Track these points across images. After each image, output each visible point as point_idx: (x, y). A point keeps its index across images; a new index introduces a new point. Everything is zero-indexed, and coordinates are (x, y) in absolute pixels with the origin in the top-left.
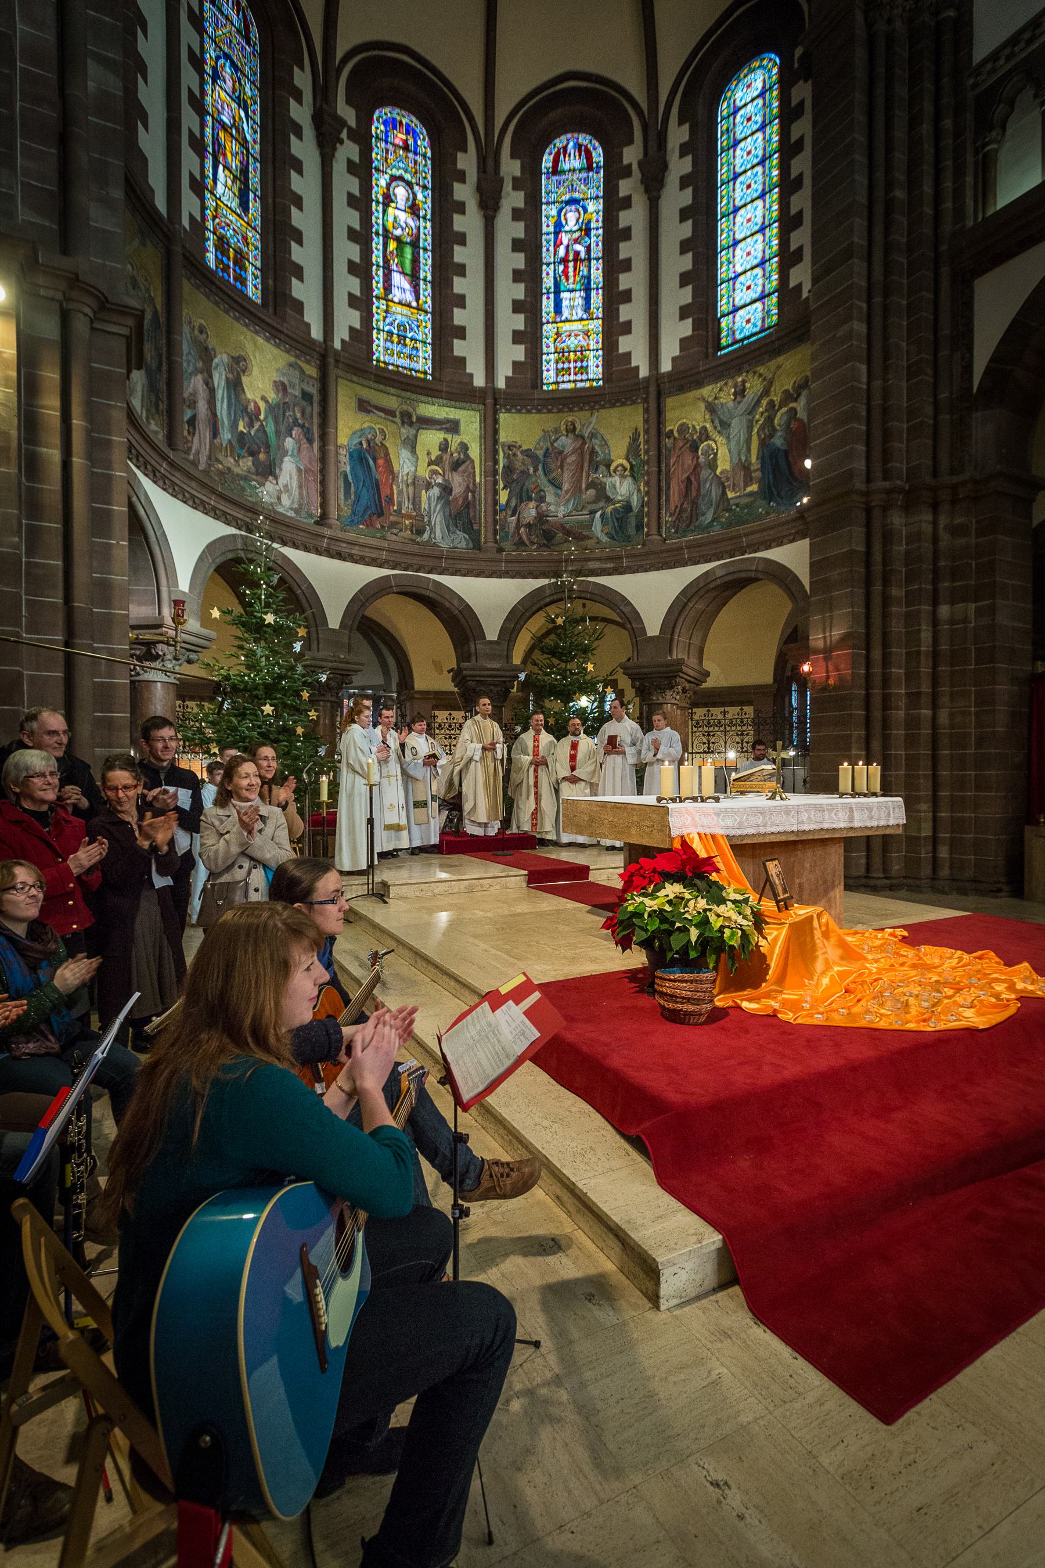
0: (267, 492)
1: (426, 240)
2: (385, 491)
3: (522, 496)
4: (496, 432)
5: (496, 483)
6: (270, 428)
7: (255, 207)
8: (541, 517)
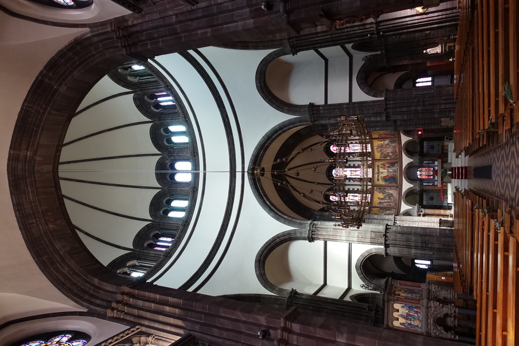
0: (395, 195)
1: (350, 169)
2: (390, 177)
3: (388, 156)
4: (378, 159)
5: (386, 159)
6: (386, 194)
7: (356, 195)
8: (392, 153)
